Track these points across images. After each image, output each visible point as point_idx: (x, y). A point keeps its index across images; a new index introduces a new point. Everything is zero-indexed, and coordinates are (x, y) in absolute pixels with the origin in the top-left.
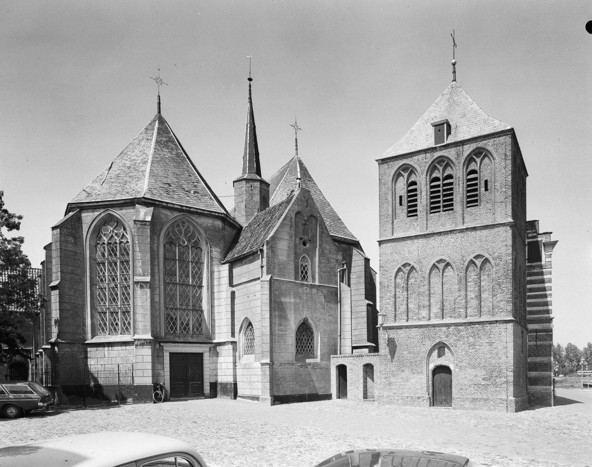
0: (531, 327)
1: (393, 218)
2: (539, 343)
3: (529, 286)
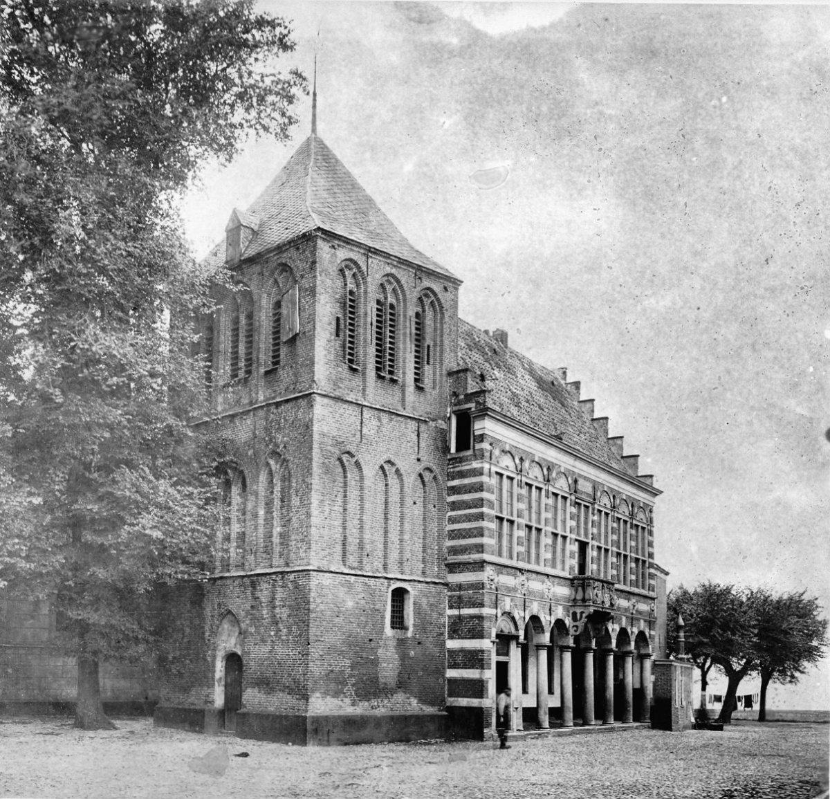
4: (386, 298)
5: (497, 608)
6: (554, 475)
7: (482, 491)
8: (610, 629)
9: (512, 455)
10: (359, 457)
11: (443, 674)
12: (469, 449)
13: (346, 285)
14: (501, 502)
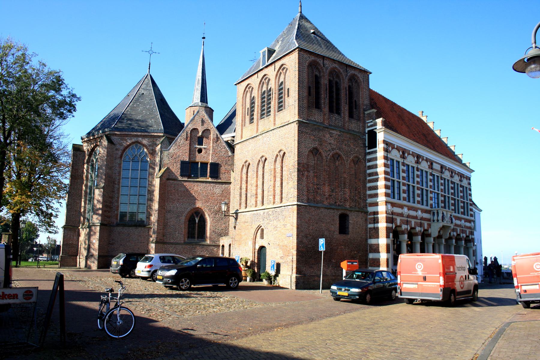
1: (242, 126)
4: (333, 78)
5: (392, 224)
6: (420, 160)
8: (452, 234)
10: (321, 150)
11: (367, 255)
13: (313, 72)
14: (393, 172)
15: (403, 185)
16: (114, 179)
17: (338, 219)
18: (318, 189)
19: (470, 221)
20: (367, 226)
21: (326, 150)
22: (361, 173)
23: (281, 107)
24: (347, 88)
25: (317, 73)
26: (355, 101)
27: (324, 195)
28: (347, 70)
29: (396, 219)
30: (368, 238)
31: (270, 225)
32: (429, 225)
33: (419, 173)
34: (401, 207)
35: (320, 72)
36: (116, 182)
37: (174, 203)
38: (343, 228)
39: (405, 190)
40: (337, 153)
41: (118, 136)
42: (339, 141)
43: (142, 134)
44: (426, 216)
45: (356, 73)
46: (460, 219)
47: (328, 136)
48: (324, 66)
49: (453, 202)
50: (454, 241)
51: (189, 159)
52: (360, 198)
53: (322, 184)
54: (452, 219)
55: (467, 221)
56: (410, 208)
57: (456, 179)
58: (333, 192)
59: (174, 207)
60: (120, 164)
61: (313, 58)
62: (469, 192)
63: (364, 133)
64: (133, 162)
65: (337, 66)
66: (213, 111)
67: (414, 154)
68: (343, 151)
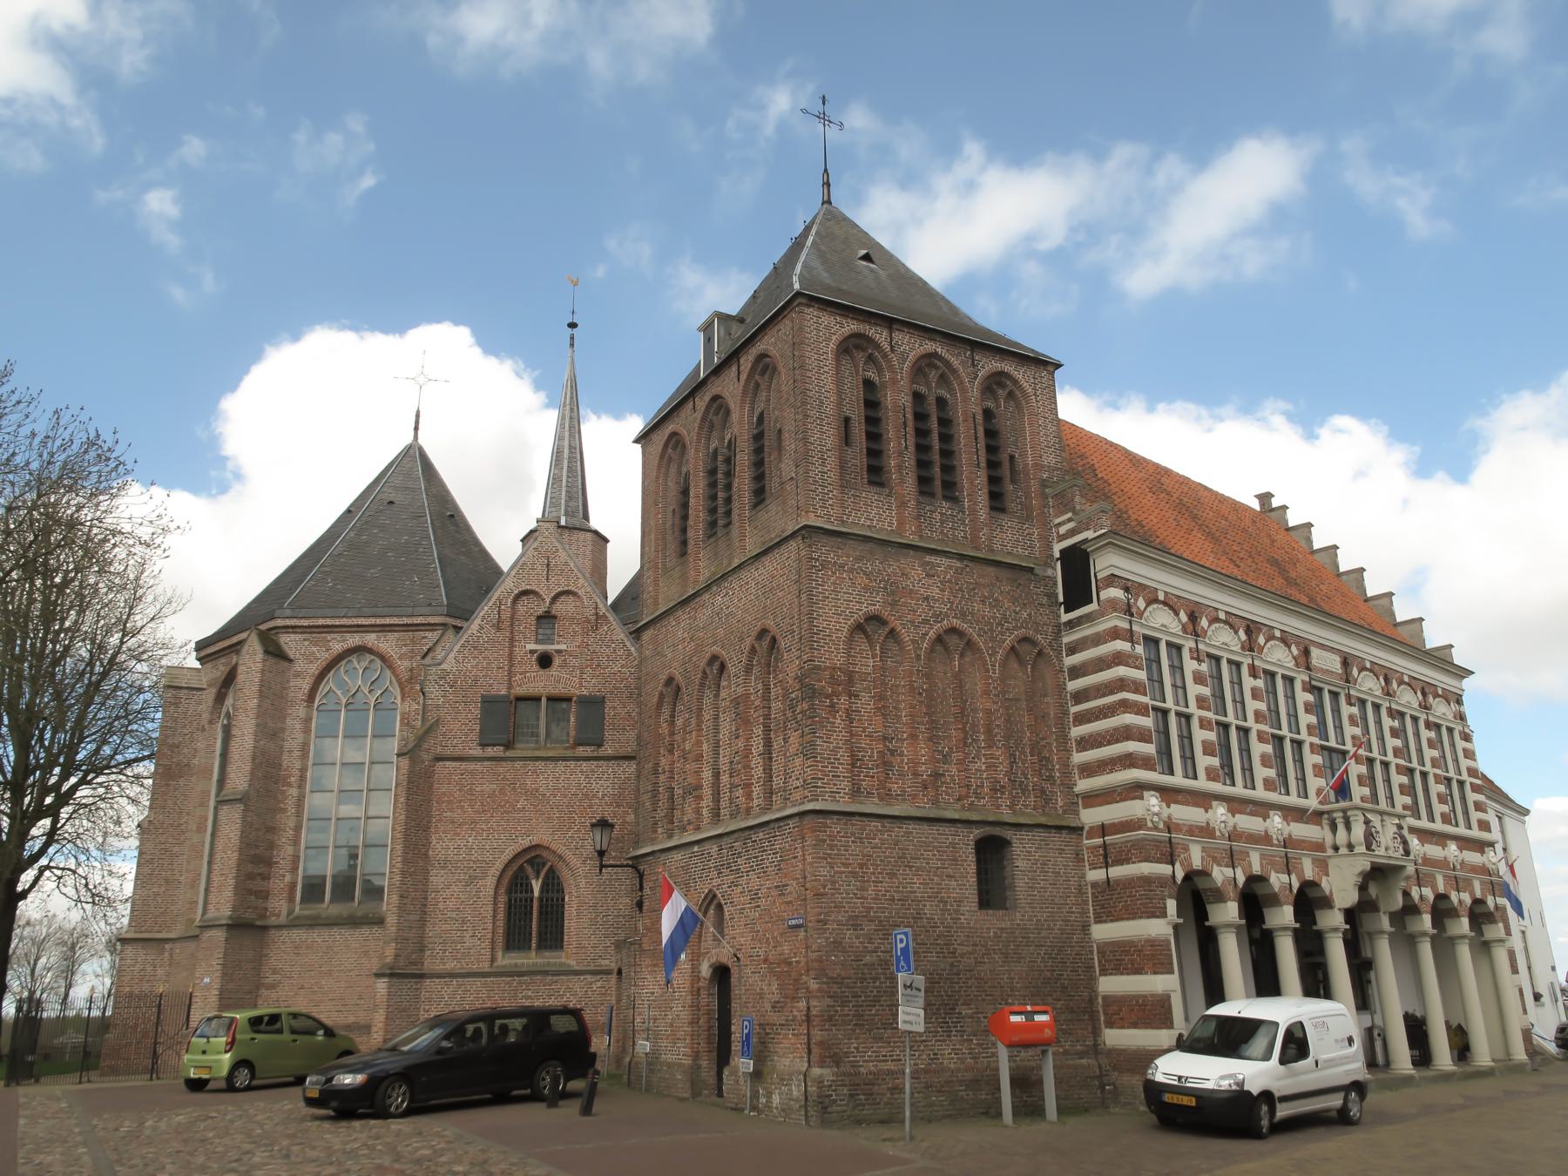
0: (1091, 816)
2: (1117, 872)
3: (1073, 685)
4: (930, 389)
6: (1261, 640)
7: (1118, 664)
8: (1415, 893)
9: (1171, 608)
10: (895, 623)
12: (1091, 602)
15: (1202, 727)
16: (285, 770)
17: (972, 858)
18: (892, 754)
19: (1481, 846)
20: (1083, 876)
21: (912, 622)
22: (1046, 695)
23: (760, 495)
24: (980, 418)
25: (871, 374)
26: (1012, 457)
27: (916, 774)
28: (973, 360)
29: (1186, 849)
30: (1092, 919)
31: (739, 889)
32: (1322, 866)
33: (1260, 683)
34: (1203, 799)
35: (880, 370)
36: (293, 779)
37: (458, 835)
38: (992, 891)
39: (1212, 743)
40: (953, 630)
41: (301, 633)
42: (961, 589)
43: (379, 621)
44: (1301, 830)
45: (1008, 367)
46: (1441, 839)
47: (917, 572)
48: (892, 350)
49: (1404, 780)
50: (1427, 919)
51: (510, 687)
52: (1051, 778)
53: (905, 735)
54: (1405, 842)
55: (1466, 843)
56: (1237, 805)
57: (1407, 699)
58: (950, 764)
59: (459, 848)
60: (308, 720)
61: (852, 326)
62: (1461, 744)
63: (1048, 561)
64: (349, 713)
65: (939, 350)
66: (606, 541)
67: (1231, 621)
68: (978, 622)
